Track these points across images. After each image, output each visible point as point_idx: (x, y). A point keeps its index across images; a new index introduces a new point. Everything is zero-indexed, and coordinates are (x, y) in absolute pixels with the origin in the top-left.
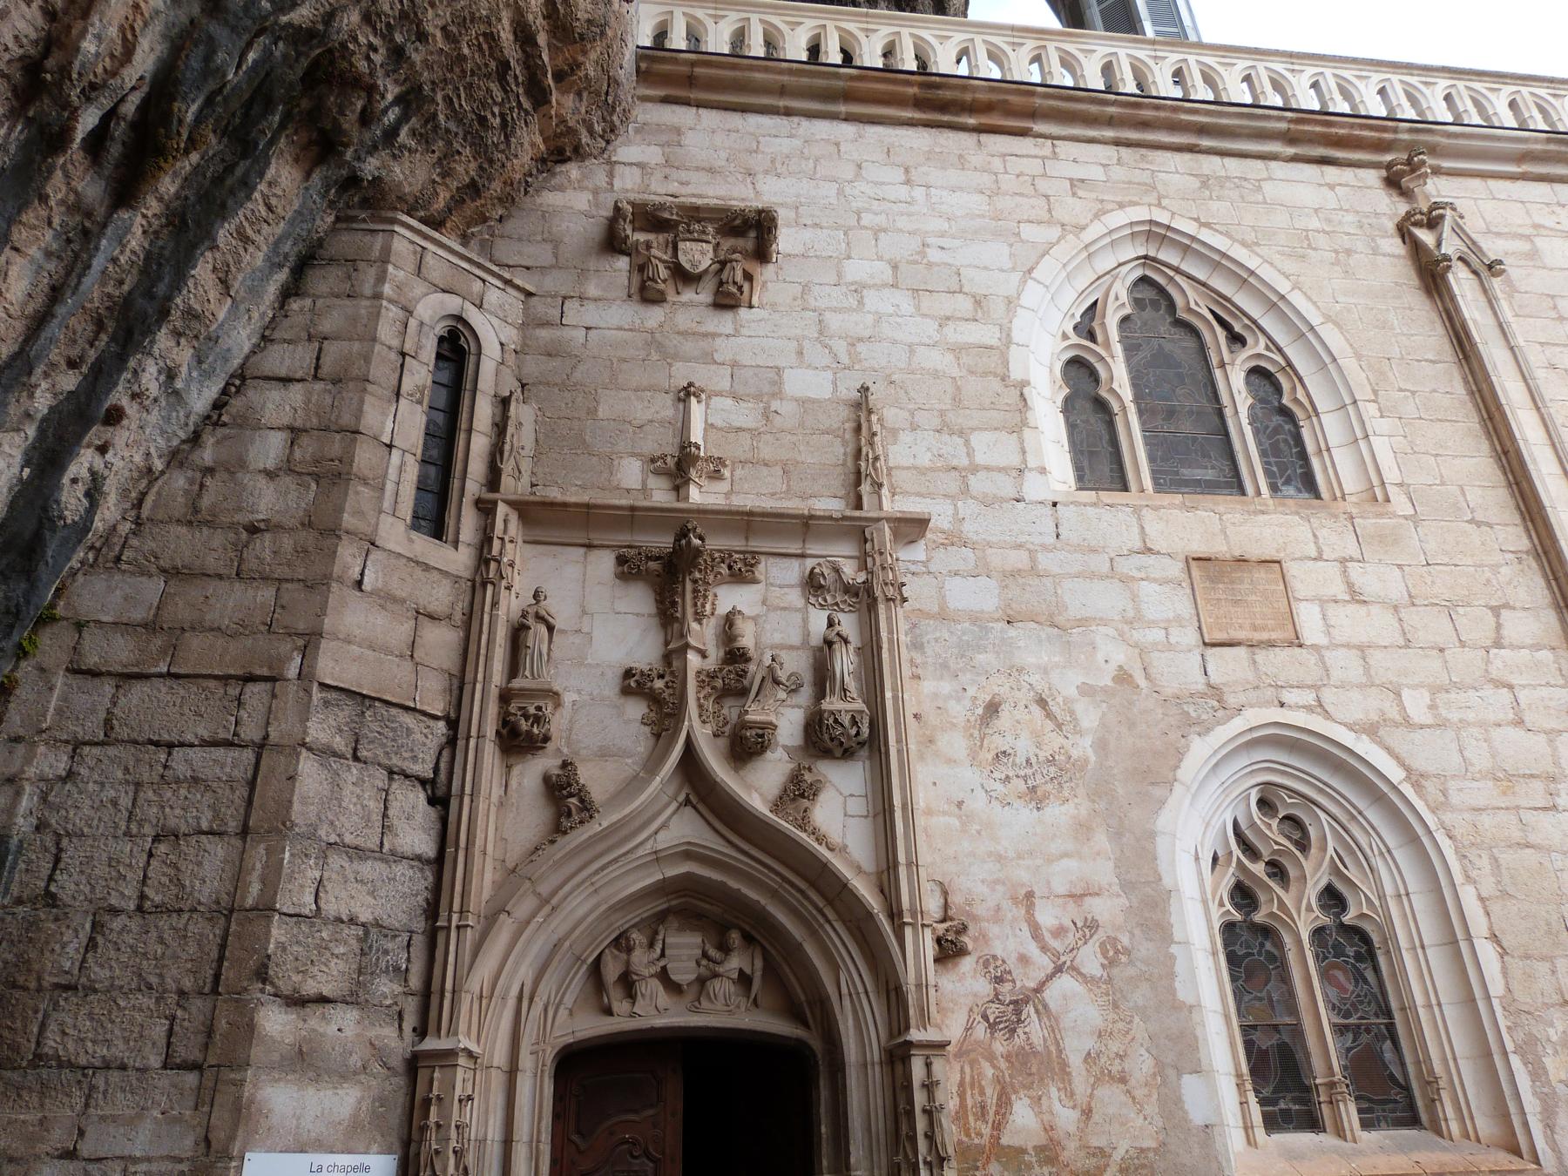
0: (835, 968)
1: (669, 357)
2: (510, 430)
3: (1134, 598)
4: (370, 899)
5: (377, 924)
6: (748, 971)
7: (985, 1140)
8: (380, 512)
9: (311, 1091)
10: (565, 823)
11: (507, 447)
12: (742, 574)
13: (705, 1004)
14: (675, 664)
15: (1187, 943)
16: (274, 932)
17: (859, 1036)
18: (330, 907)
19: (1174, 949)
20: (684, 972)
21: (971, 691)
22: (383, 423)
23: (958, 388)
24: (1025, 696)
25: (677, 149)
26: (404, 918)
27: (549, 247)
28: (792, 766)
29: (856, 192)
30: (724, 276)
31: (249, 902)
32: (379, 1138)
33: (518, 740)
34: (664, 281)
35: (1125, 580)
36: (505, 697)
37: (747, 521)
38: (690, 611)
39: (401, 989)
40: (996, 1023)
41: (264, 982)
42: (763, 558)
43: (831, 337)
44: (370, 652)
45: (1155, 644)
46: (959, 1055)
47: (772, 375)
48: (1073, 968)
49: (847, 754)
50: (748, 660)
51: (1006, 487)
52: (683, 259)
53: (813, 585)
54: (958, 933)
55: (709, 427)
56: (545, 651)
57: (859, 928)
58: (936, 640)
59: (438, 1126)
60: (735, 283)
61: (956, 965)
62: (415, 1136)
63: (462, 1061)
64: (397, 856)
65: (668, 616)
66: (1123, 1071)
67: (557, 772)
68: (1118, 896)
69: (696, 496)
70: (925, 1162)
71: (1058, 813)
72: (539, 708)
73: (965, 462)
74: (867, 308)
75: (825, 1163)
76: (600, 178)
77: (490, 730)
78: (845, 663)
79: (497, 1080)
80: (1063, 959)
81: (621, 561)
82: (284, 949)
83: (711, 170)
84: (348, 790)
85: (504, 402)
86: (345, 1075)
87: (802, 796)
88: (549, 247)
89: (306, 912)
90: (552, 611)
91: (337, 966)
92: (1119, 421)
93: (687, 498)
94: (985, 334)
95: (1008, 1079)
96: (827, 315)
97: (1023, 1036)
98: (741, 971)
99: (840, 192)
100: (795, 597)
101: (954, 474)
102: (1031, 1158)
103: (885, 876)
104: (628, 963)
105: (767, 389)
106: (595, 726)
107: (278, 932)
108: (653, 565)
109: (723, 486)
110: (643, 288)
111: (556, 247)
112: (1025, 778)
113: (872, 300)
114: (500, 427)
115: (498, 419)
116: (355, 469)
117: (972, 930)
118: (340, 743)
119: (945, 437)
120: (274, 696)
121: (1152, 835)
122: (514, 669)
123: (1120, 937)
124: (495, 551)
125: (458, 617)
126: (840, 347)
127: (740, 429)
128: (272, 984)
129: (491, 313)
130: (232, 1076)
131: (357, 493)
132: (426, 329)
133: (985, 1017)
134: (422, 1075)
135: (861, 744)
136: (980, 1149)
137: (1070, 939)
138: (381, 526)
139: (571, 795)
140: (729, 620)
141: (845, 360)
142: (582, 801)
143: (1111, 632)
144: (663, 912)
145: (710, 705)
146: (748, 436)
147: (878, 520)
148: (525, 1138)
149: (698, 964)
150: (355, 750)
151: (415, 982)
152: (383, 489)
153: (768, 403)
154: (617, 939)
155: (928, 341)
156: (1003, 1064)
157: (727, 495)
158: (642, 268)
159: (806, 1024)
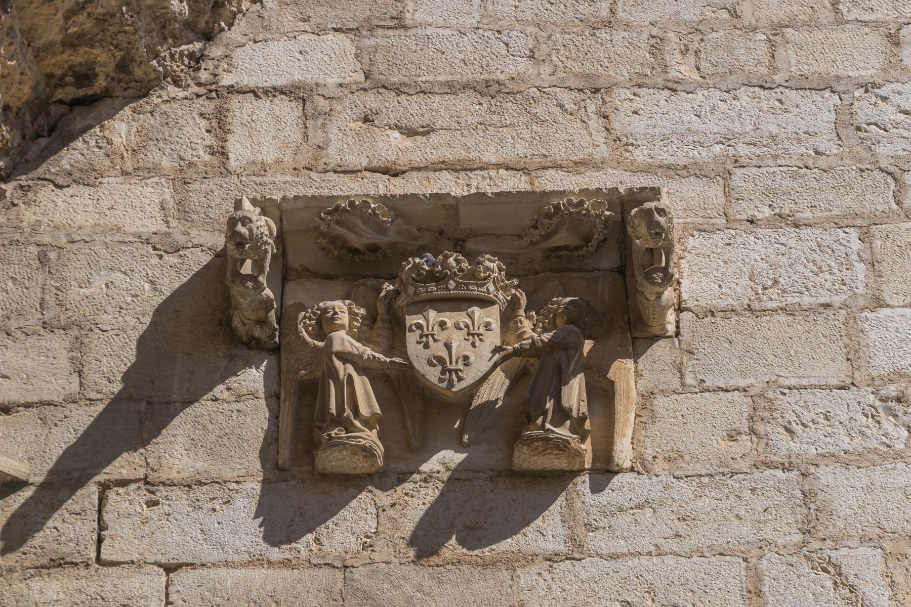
25: (396, 38)
29: (889, 113)
43: (838, 541)
76: (194, 135)
83: (488, 89)
88: (59, 344)
96: (825, 474)
99: (846, 123)
111: (79, 344)
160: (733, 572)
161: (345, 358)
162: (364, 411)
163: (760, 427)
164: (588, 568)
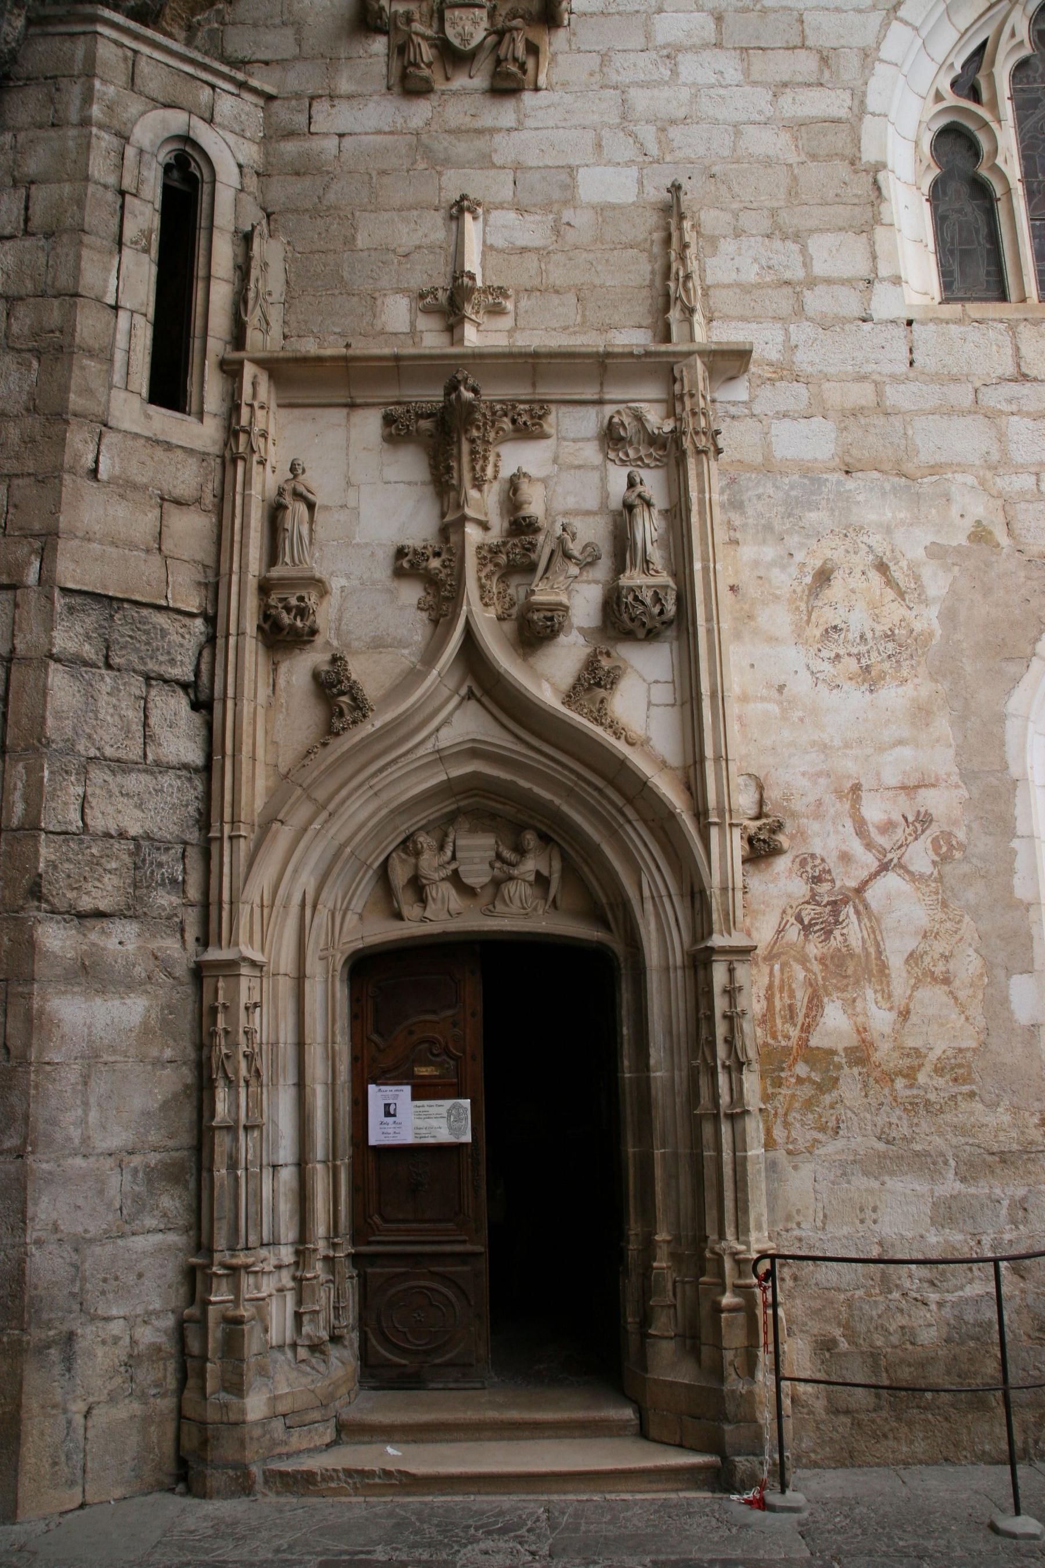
0: (636, 870)
1: (439, 163)
2: (254, 273)
3: (1001, 438)
4: (138, 814)
5: (148, 837)
6: (546, 873)
7: (793, 1042)
8: (111, 387)
9: (98, 1001)
10: (338, 724)
11: (251, 295)
12: (528, 428)
13: (500, 907)
14: (453, 538)
15: (1031, 837)
16: (43, 851)
17: (660, 941)
18: (98, 822)
19: (1015, 844)
20: (477, 875)
21: (799, 557)
22: (106, 281)
23: (795, 179)
24: (863, 560)
26: (175, 829)
27: (289, 32)
28: (588, 650)
30: (502, 52)
31: (15, 822)
32: (171, 1042)
33: (281, 636)
34: (429, 65)
35: (991, 416)
36: (265, 588)
37: (532, 365)
38: (467, 477)
39: (179, 901)
40: (810, 925)
41: (39, 899)
42: (553, 408)
43: (636, 122)
44: (114, 550)
45: (1022, 493)
46: (770, 958)
47: (564, 177)
48: (900, 866)
49: (651, 635)
50: (537, 530)
51: (849, 303)
52: (450, 33)
53: (611, 438)
54: (773, 831)
55: (488, 249)
56: (305, 532)
57: (663, 828)
58: (759, 497)
59: (227, 1032)
60: (515, 59)
61: (769, 865)
62: (206, 1041)
63: (245, 970)
64: (162, 767)
65: (443, 484)
66: (948, 972)
67: (326, 667)
68: (957, 786)
69: (472, 337)
70: (724, 1066)
71: (894, 696)
72: (301, 599)
73: (800, 274)
74: (682, 78)
75: (626, 1063)
77: (250, 625)
78: (649, 529)
79: (285, 987)
80: (889, 856)
81: (389, 420)
82: (55, 867)
84: (103, 700)
85: (247, 239)
86: (128, 985)
87: (598, 685)
89: (74, 829)
90: (313, 486)
91: (110, 881)
92: (1001, 208)
93: (461, 340)
94: (830, 103)
95: (820, 982)
96: (633, 92)
97: (839, 938)
98: (538, 874)
100: (591, 452)
101: (787, 290)
102: (841, 1059)
103: (692, 770)
104: (416, 867)
105: (556, 195)
106: (368, 616)
107: (46, 852)
108: (425, 424)
109: (506, 322)
110: (404, 77)
112: (858, 657)
113: (688, 65)
114: (243, 270)
115: (240, 260)
116: (77, 340)
117: (789, 827)
118: (89, 651)
119: (777, 244)
120: (16, 605)
121: (1001, 718)
122: (273, 556)
123: (955, 831)
124: (244, 421)
125: (209, 499)
126: (648, 133)
127: (524, 250)
128: (47, 901)
129: (224, 128)
130: (20, 989)
131: (83, 368)
132: (146, 157)
133: (799, 919)
134: (208, 983)
135: (667, 624)
136: (787, 1051)
137: (899, 835)
138: (113, 404)
139: (342, 693)
140: (514, 484)
141: (653, 149)
142: (354, 699)
143: (970, 479)
144: (452, 812)
145: (494, 586)
146: (534, 257)
147: (689, 354)
148: (319, 1038)
149: (492, 867)
150: (107, 657)
151: (194, 893)
152: (111, 360)
153: (559, 212)
154: (404, 842)
155: (757, 118)
156: (816, 967)
157: (511, 332)
158: (402, 50)
159: (607, 927)
160: (589, 136)
161: (417, 34)
162: (425, 59)
163: (605, 70)
164: (524, 135)
